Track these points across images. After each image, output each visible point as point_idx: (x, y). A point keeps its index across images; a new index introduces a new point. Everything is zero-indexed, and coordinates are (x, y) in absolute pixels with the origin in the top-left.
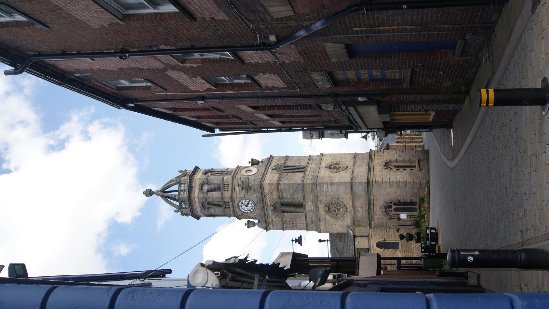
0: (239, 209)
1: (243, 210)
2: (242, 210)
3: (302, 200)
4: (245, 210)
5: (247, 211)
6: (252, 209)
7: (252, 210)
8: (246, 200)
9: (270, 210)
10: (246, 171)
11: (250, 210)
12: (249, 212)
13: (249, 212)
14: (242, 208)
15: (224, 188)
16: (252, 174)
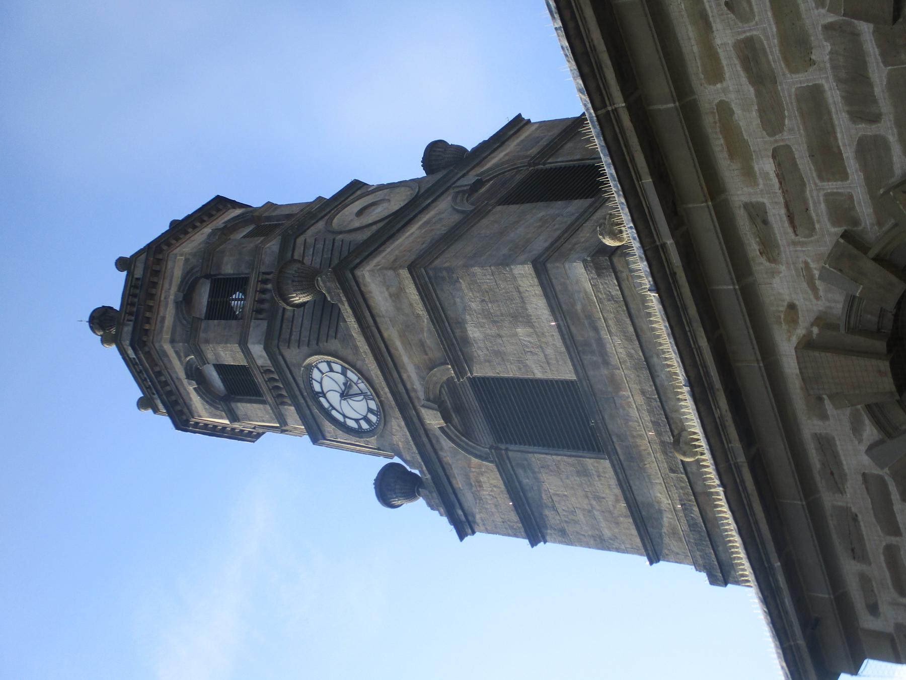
0: (321, 406)
1: (340, 418)
2: (334, 413)
3: (567, 373)
4: (345, 416)
5: (357, 421)
6: (370, 410)
7: (373, 418)
8: (344, 368)
9: (433, 420)
10: (360, 213)
11: (366, 419)
12: (365, 426)
13: (365, 426)
14: (334, 408)
15: (261, 301)
16: (370, 222)
